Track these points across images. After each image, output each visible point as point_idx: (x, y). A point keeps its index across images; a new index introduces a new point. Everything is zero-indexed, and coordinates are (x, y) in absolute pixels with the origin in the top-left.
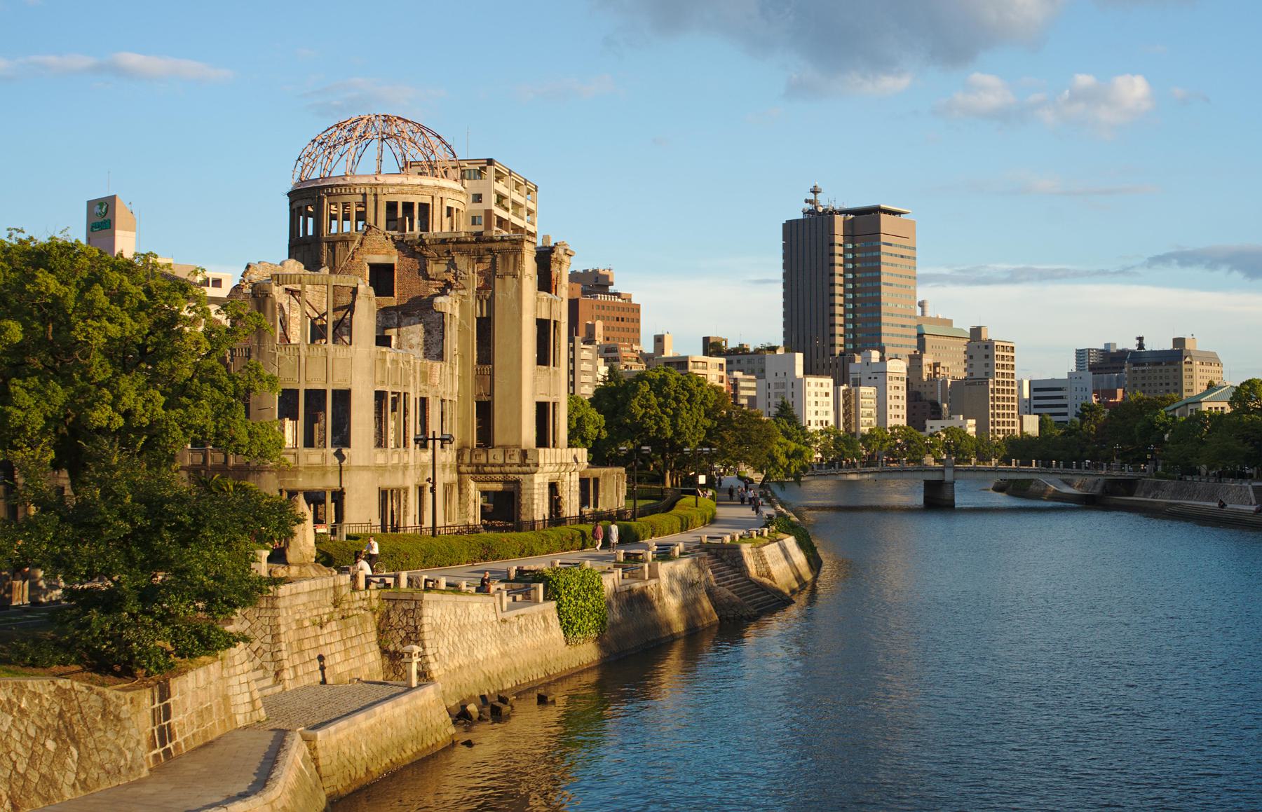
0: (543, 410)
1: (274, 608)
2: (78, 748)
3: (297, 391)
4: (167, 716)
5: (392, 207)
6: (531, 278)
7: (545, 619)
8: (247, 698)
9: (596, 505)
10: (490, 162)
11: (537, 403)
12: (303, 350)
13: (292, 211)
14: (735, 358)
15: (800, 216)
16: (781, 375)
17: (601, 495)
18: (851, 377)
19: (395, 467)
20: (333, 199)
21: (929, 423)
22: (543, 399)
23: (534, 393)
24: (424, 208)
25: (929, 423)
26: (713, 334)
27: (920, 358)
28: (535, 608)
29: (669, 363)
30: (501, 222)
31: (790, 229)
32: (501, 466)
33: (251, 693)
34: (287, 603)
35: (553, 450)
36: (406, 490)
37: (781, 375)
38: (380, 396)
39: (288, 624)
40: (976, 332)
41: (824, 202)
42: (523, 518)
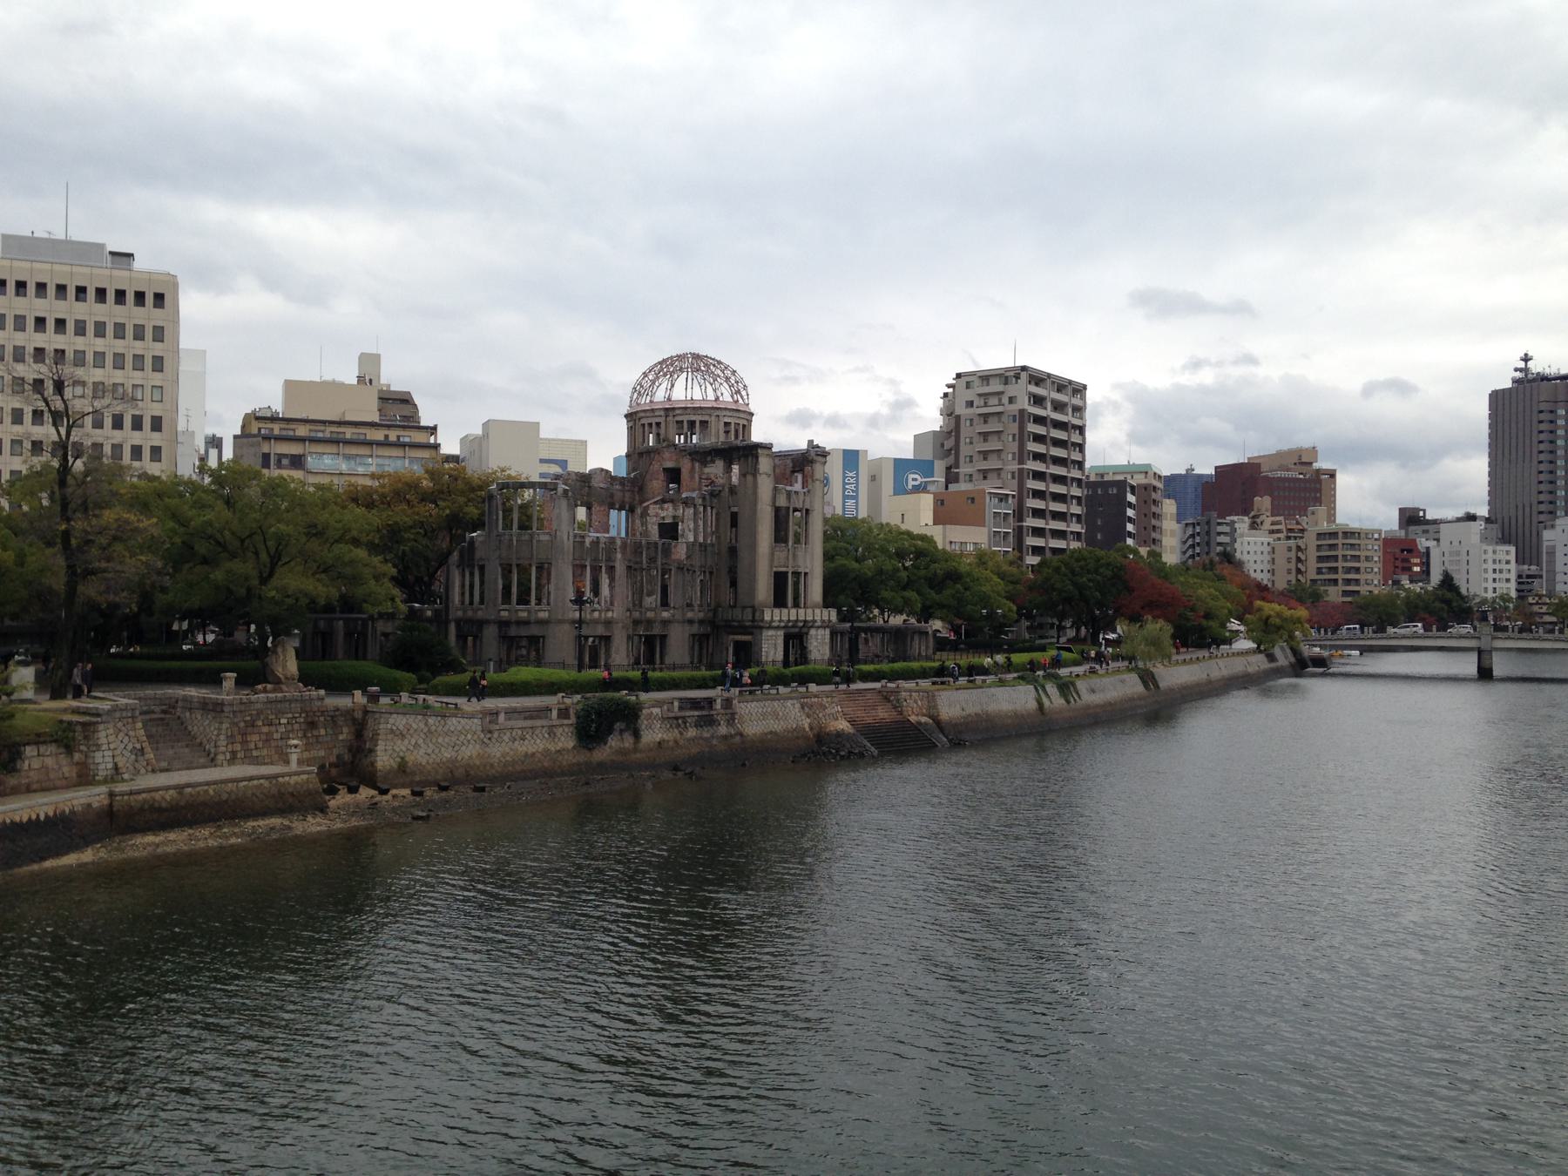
5: (680, 423)
6: (769, 476)
8: (110, 766)
10: (1024, 368)
11: (776, 573)
15: (1508, 384)
16: (1456, 543)
18: (1545, 544)
20: (643, 421)
23: (771, 567)
24: (704, 424)
30: (1039, 420)
31: (1497, 398)
32: (739, 621)
33: (116, 764)
37: (1456, 543)
41: (1536, 367)
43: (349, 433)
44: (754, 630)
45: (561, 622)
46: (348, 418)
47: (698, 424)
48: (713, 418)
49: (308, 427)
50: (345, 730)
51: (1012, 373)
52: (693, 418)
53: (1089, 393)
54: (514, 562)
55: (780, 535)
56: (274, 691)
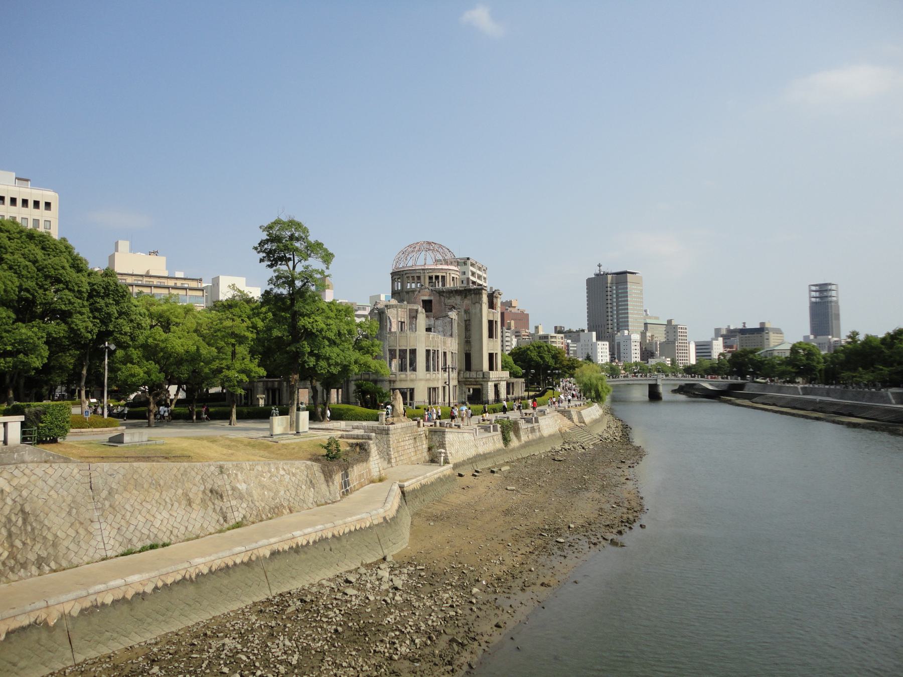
0: (491, 356)
1: (388, 434)
2: (314, 489)
3: (396, 350)
4: (347, 477)
7: (493, 439)
8: (378, 470)
9: (513, 394)
10: (468, 259)
12: (398, 333)
13: (392, 280)
14: (567, 334)
17: (515, 389)
19: (434, 380)
20: (408, 275)
21: (650, 360)
22: (492, 352)
23: (488, 350)
24: (443, 277)
25: (650, 360)
26: (558, 325)
27: (646, 333)
28: (489, 434)
29: (542, 337)
30: (474, 283)
34: (393, 432)
35: (496, 372)
36: (438, 388)
38: (428, 351)
39: (393, 441)
40: (670, 322)
41: (604, 269)
42: (484, 399)
43: (156, 282)
44: (483, 383)
45: (421, 380)
46: (152, 273)
47: (440, 278)
48: (448, 275)
49: (134, 278)
50: (424, 442)
51: (463, 261)
52: (438, 274)
53: (487, 271)
54: (398, 348)
55: (491, 336)
56: (398, 421)
